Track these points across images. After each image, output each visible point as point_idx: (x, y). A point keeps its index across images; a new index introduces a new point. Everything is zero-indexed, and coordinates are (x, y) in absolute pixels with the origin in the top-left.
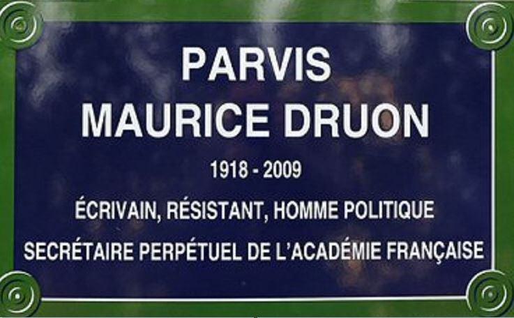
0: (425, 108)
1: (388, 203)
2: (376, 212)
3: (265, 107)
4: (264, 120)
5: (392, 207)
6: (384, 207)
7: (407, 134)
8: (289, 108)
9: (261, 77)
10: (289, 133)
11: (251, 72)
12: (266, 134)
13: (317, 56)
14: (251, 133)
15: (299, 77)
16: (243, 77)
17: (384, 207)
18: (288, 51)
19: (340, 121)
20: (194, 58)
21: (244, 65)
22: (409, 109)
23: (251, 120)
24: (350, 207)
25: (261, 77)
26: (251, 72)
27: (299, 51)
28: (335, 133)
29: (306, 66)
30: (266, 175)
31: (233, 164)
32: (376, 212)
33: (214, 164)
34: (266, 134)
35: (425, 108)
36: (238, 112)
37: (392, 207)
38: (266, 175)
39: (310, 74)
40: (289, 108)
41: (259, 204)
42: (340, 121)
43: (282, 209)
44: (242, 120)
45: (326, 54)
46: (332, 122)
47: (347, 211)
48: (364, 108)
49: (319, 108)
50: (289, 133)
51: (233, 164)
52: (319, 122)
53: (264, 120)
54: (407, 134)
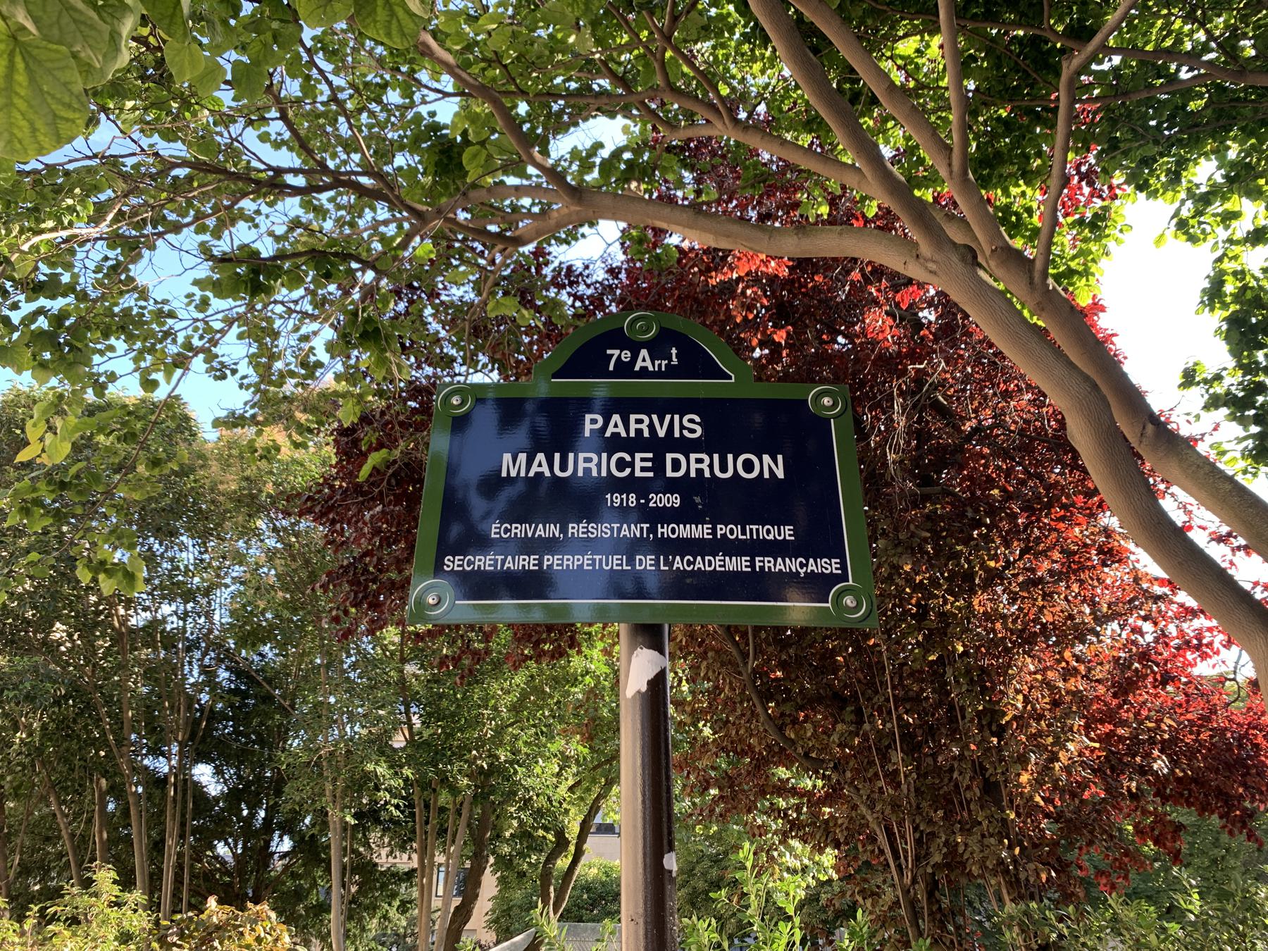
0: (780, 458)
1: (754, 527)
2: (744, 533)
3: (650, 455)
4: (649, 464)
5: (757, 530)
6: (751, 530)
7: (766, 475)
8: (669, 457)
9: (646, 434)
10: (669, 474)
11: (639, 432)
12: (651, 474)
13: (691, 421)
14: (638, 474)
15: (677, 434)
16: (632, 434)
17: (751, 530)
18: (668, 417)
19: (711, 466)
20: (594, 421)
21: (633, 426)
22: (766, 458)
23: (638, 464)
24: (721, 530)
25: (646, 434)
26: (639, 432)
27: (677, 417)
28: (707, 474)
29: (682, 427)
30: (651, 504)
31: (624, 496)
32: (744, 533)
33: (608, 496)
34: (651, 474)
35: (780, 458)
36: (628, 458)
37: (757, 530)
38: (651, 504)
39: (686, 433)
40: (669, 457)
41: (645, 526)
42: (711, 466)
43: (665, 530)
44: (631, 465)
45: (697, 419)
46: (705, 466)
47: (719, 533)
48: (730, 457)
49: (693, 456)
50: (669, 474)
51: (624, 496)
52: (694, 466)
53: (649, 464)
54: (766, 475)
